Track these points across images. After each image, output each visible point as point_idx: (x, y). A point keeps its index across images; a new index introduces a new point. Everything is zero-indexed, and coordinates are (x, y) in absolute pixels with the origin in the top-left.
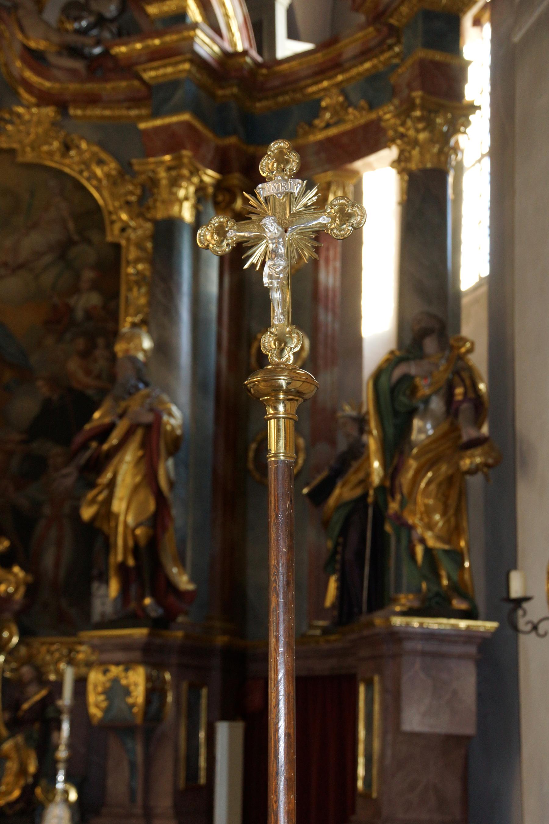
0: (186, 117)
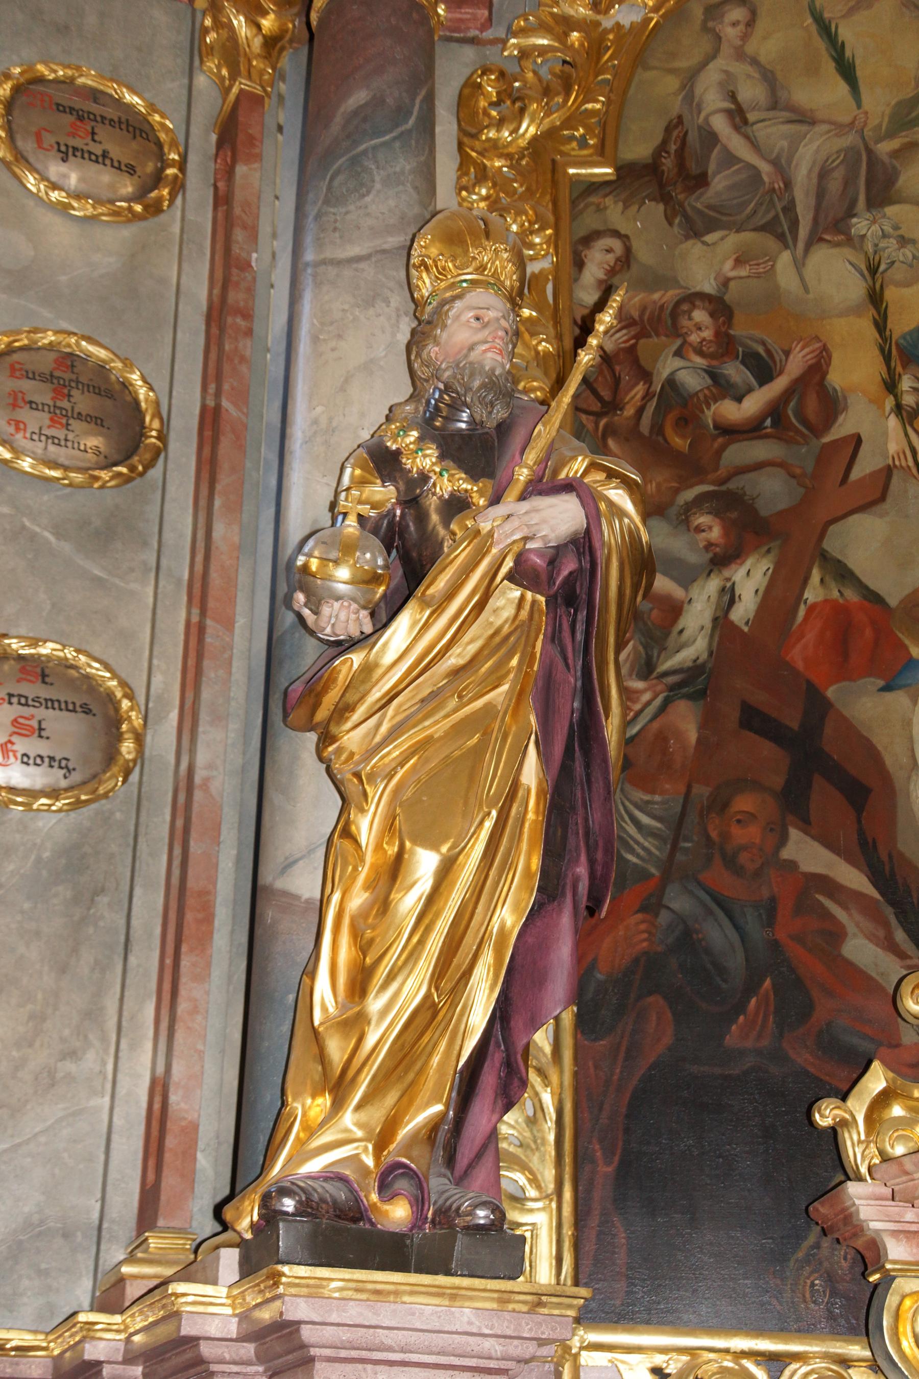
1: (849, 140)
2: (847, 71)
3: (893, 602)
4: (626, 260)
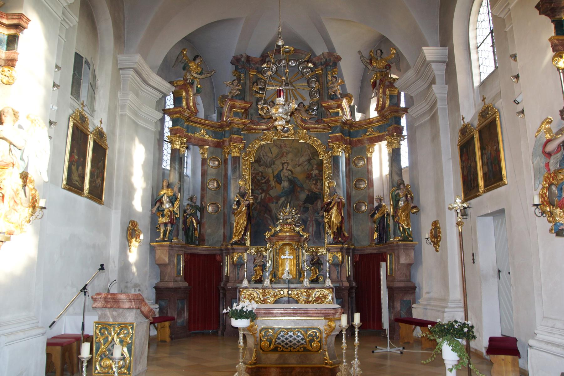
1: (271, 159)
2: (272, 153)
3: (273, 196)
4: (255, 168)
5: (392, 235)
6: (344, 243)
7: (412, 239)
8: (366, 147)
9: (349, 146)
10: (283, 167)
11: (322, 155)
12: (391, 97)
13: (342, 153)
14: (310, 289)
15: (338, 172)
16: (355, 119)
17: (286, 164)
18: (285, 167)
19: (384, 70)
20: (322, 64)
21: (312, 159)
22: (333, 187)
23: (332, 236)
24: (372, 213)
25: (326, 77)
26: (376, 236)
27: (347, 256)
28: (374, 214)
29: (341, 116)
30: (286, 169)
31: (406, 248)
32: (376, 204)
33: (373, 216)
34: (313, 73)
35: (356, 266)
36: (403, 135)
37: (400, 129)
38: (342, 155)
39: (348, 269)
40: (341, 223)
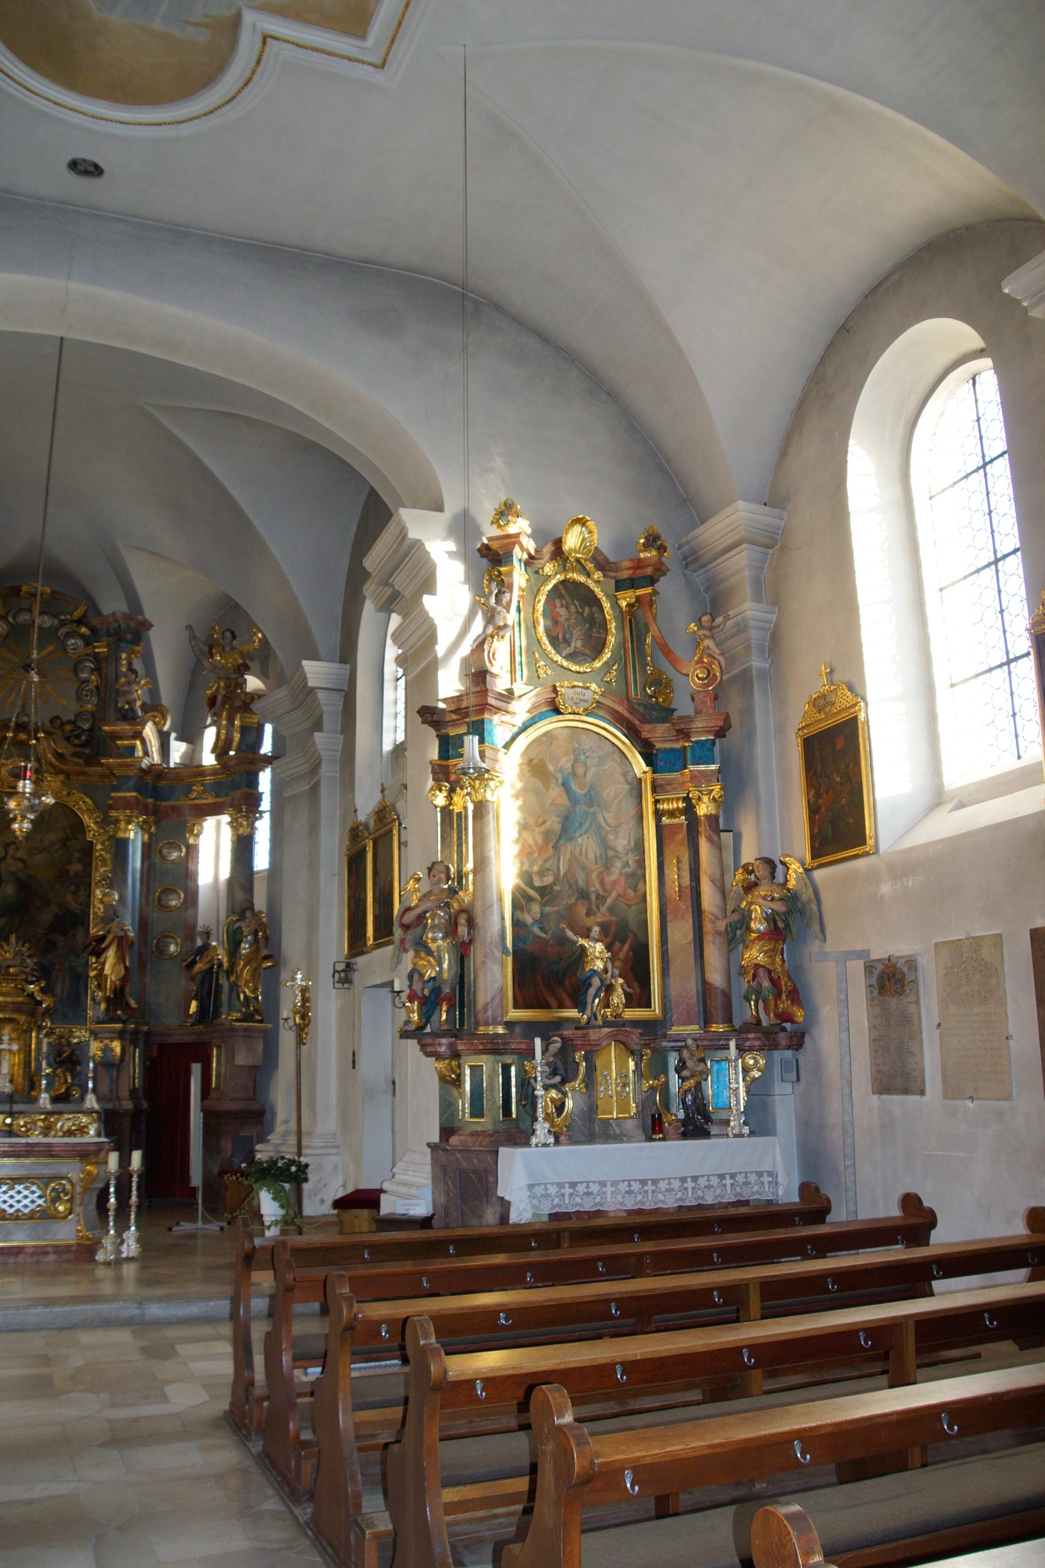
0: (134, 794)
5: (224, 1009)
6: (128, 1020)
7: (260, 1018)
8: (186, 822)
9: (151, 819)
10: (6, 853)
11: (92, 833)
12: (244, 730)
13: (136, 833)
14: (51, 1113)
15: (125, 872)
16: (168, 763)
17: (13, 846)
18: (11, 852)
19: (235, 676)
20: (109, 635)
21: (70, 839)
22: (112, 905)
23: (103, 1006)
24: (189, 960)
25: (116, 665)
26: (194, 1006)
27: (132, 1047)
28: (193, 963)
29: (139, 757)
30: (13, 857)
31: (248, 1033)
32: (199, 943)
33: (191, 965)
34: (89, 650)
35: (150, 1068)
36: (260, 809)
37: (257, 798)
38: (134, 835)
39: (134, 1073)
40: (124, 979)
